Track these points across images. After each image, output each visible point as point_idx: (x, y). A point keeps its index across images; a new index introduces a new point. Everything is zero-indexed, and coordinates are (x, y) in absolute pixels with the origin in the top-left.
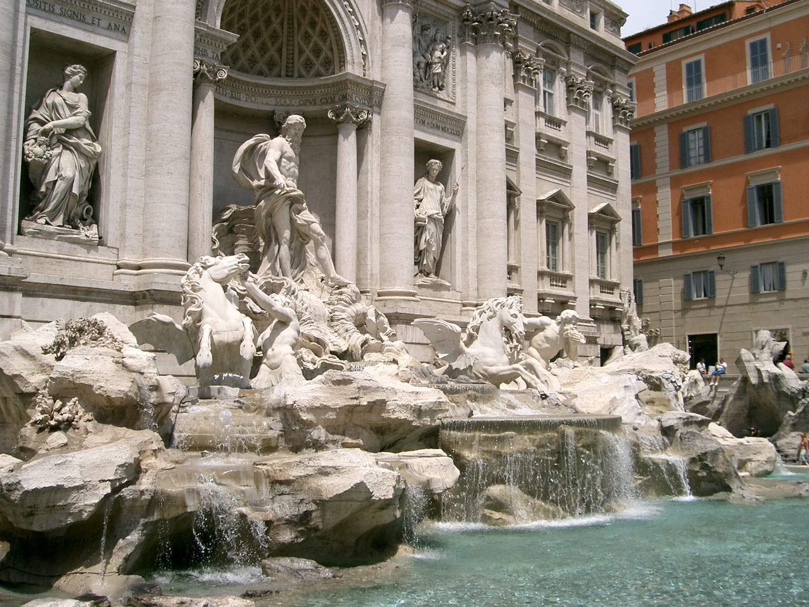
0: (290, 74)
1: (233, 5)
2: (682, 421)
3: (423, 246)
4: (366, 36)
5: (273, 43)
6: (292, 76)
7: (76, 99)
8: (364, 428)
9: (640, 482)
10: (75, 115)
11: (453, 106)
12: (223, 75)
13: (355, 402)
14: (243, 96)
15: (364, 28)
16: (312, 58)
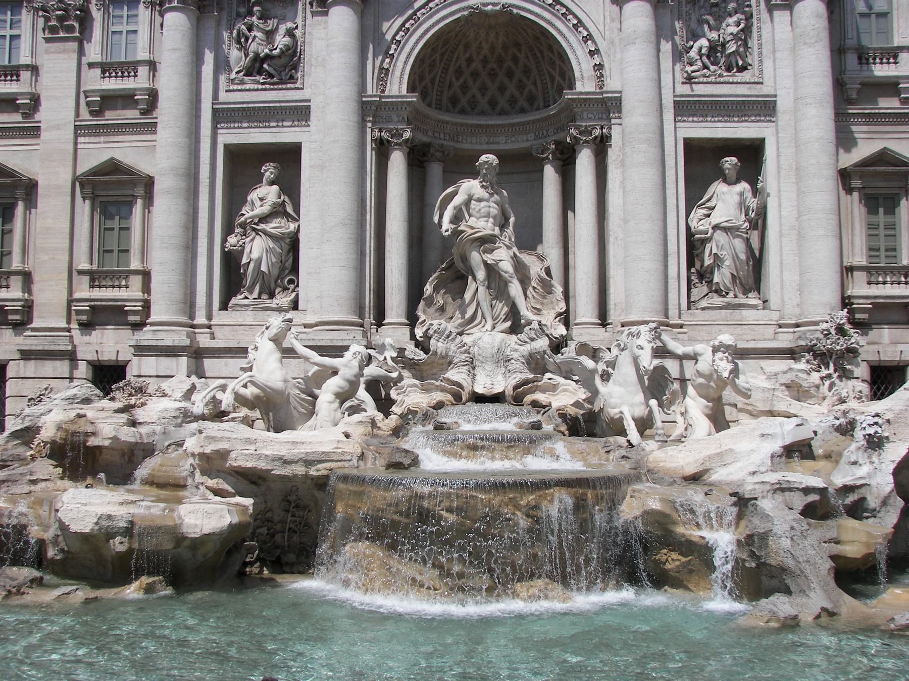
0: (547, 104)
1: (467, 55)
2: (768, 487)
3: (708, 261)
4: (602, 45)
5: (528, 78)
6: (549, 106)
7: (266, 192)
8: (230, 474)
9: (677, 563)
10: (262, 206)
11: (759, 86)
12: (407, 135)
13: (201, 450)
14: (502, 139)
15: (595, 37)
16: (562, 82)
